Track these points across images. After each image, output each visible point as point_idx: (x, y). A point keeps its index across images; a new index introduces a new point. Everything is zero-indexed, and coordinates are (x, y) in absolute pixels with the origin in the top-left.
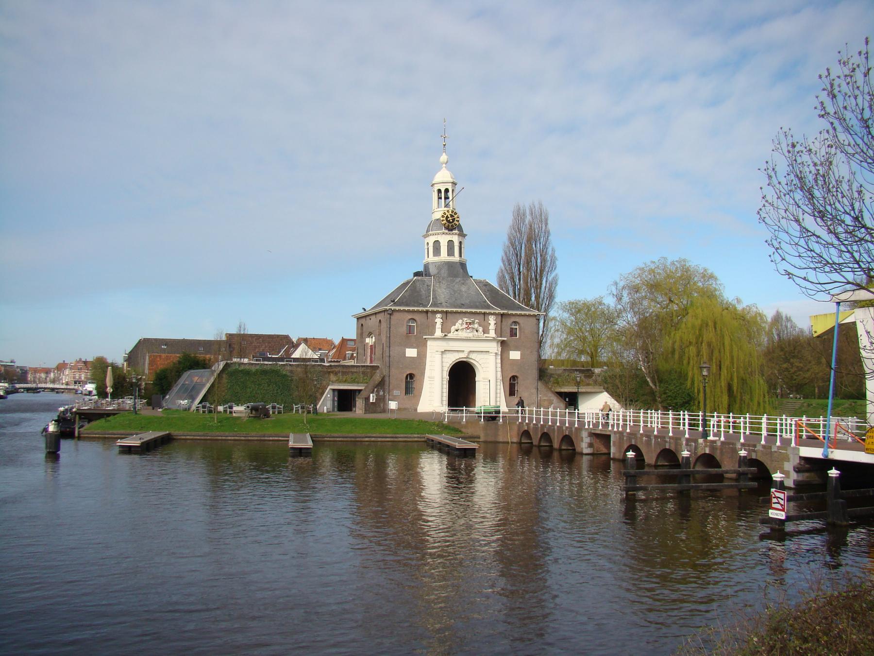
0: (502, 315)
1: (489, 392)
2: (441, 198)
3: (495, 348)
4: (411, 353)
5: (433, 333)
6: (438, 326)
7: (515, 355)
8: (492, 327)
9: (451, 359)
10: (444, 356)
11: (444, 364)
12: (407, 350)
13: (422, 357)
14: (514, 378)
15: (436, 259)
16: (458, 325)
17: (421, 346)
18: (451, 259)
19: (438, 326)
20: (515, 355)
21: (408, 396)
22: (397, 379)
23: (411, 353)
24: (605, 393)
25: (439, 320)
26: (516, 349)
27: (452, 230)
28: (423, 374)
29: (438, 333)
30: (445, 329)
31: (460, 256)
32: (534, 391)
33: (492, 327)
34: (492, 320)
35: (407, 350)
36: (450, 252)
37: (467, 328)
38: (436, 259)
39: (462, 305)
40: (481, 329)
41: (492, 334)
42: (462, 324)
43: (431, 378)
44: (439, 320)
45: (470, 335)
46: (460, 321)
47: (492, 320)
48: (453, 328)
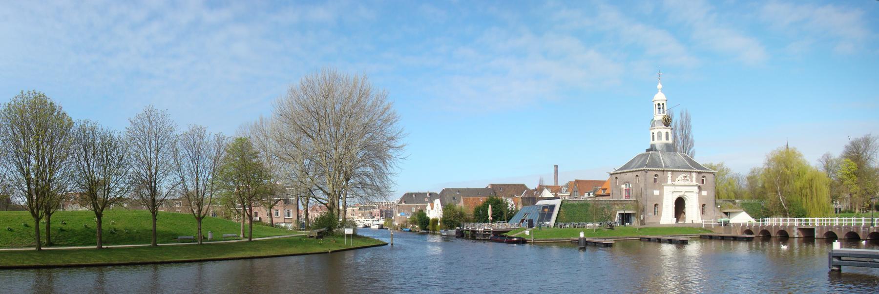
0: (699, 173)
1: (693, 215)
3: (696, 189)
4: (656, 193)
6: (669, 178)
8: (694, 178)
9: (676, 196)
13: (661, 194)
14: (704, 205)
15: (660, 142)
16: (679, 178)
17: (661, 189)
19: (669, 178)
22: (650, 206)
23: (656, 193)
24: (744, 213)
28: (662, 204)
29: (669, 182)
30: (673, 180)
34: (694, 175)
36: (667, 138)
38: (660, 142)
39: (679, 167)
41: (694, 182)
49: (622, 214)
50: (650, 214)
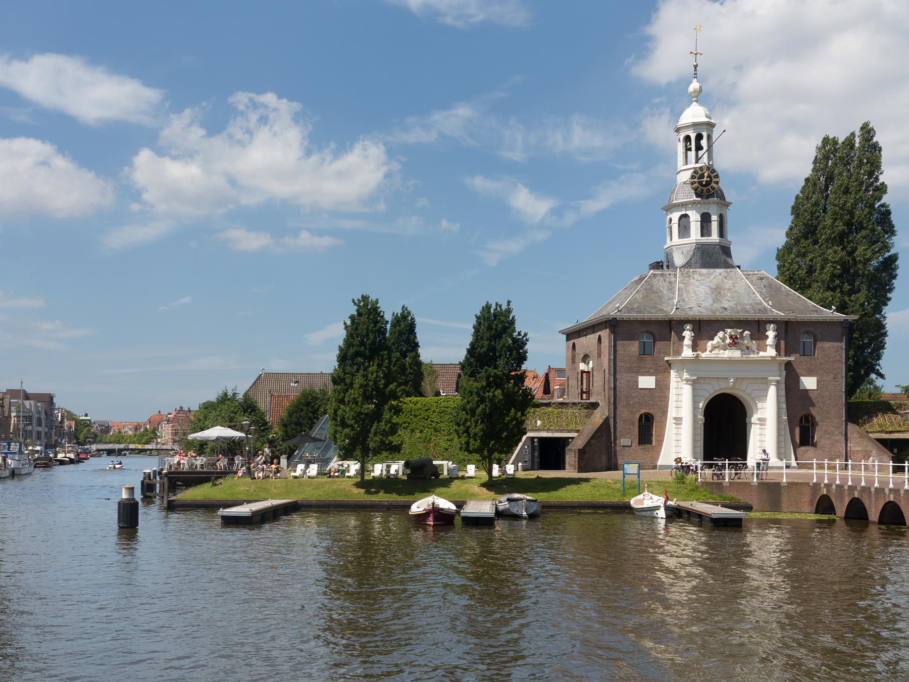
2: (690, 149)
4: (647, 382)
5: (679, 352)
6: (687, 341)
8: (770, 340)
12: (640, 378)
13: (663, 388)
17: (662, 371)
18: (705, 240)
19: (687, 341)
21: (642, 447)
23: (647, 382)
25: (688, 334)
26: (810, 374)
27: (708, 197)
31: (721, 233)
35: (640, 378)
42: (723, 339)
44: (688, 334)
46: (721, 334)
49: (542, 440)
50: (624, 441)
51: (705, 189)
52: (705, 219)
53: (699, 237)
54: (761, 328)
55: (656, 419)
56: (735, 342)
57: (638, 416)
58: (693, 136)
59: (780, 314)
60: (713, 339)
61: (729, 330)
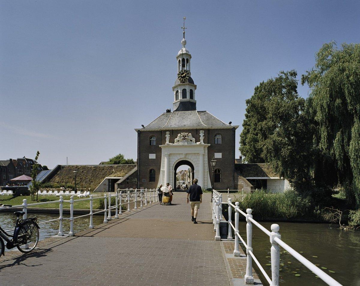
4: (152, 156)
7: (218, 155)
8: (202, 138)
9: (176, 160)
10: (171, 157)
11: (171, 162)
17: (158, 151)
18: (185, 100)
20: (218, 155)
25: (168, 136)
26: (219, 152)
29: (167, 142)
30: (172, 141)
32: (232, 178)
33: (202, 138)
34: (202, 134)
36: (184, 96)
37: (184, 139)
40: (194, 139)
42: (180, 137)
43: (164, 171)
44: (168, 136)
45: (186, 144)
46: (179, 135)
47: (202, 134)
48: (176, 140)
51: (183, 79)
52: (184, 92)
53: (182, 99)
54: (198, 132)
55: (156, 171)
56: (184, 138)
57: (149, 170)
58: (181, 59)
59: (205, 126)
60: (177, 138)
61: (182, 133)
